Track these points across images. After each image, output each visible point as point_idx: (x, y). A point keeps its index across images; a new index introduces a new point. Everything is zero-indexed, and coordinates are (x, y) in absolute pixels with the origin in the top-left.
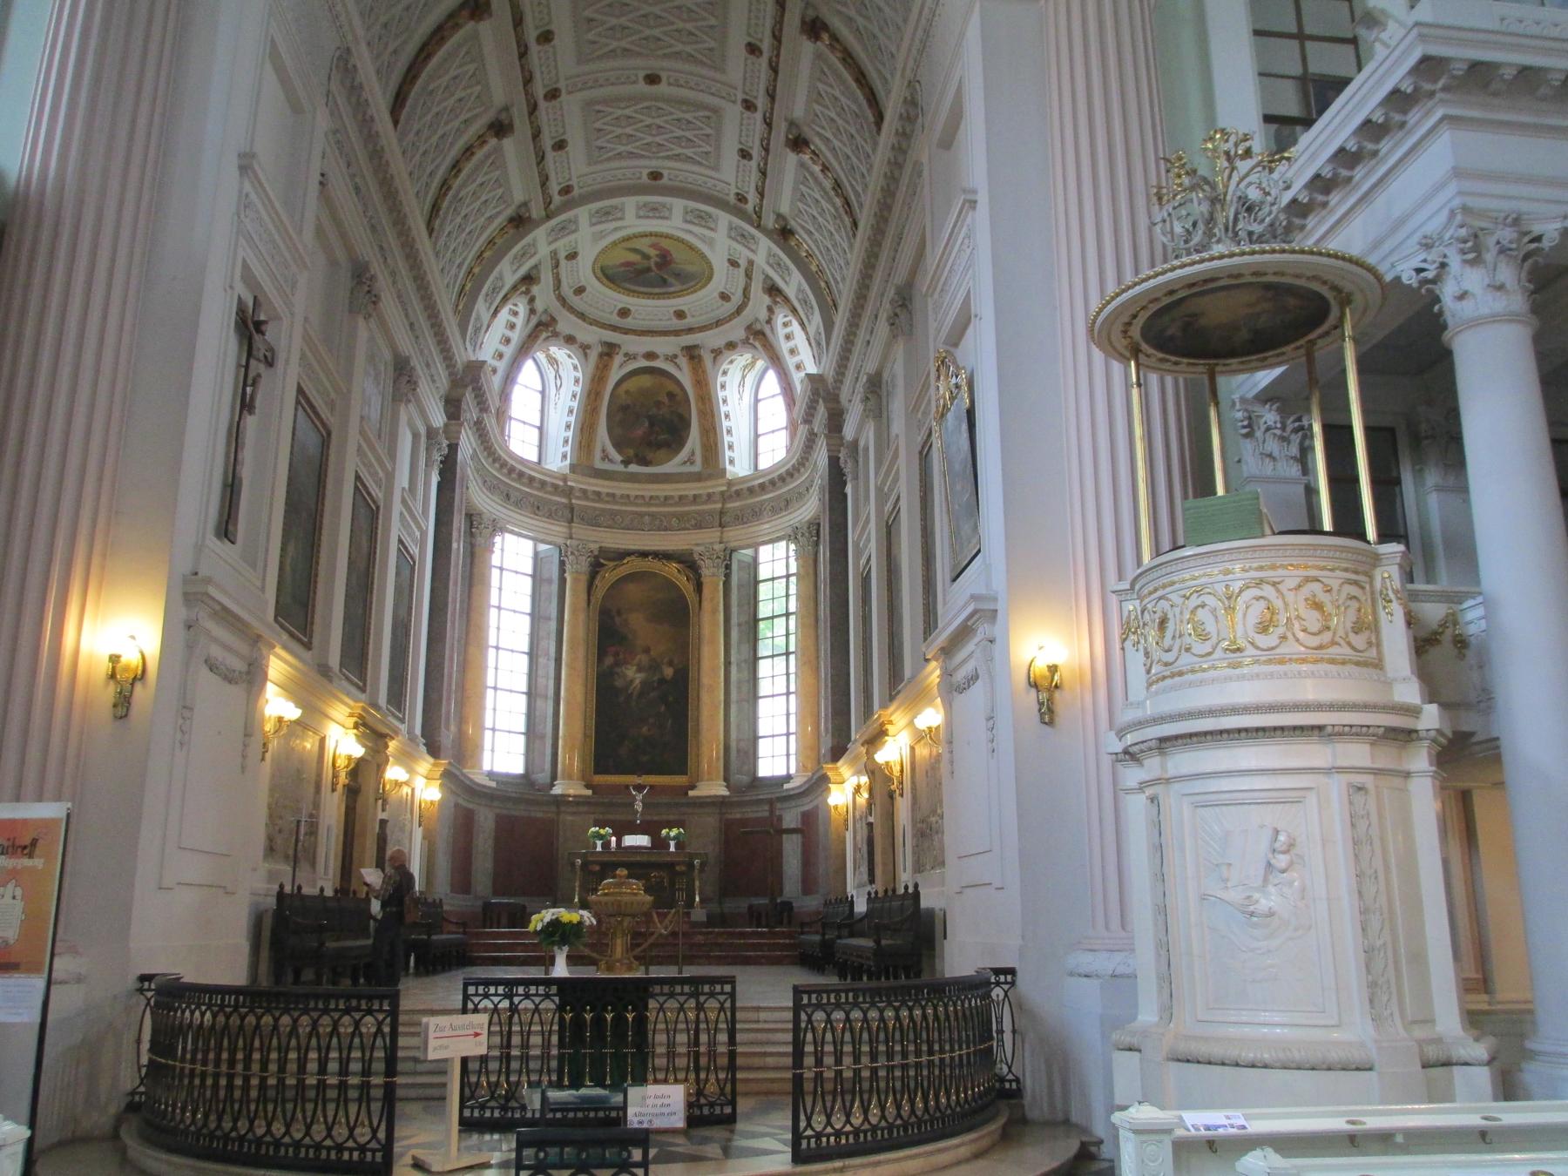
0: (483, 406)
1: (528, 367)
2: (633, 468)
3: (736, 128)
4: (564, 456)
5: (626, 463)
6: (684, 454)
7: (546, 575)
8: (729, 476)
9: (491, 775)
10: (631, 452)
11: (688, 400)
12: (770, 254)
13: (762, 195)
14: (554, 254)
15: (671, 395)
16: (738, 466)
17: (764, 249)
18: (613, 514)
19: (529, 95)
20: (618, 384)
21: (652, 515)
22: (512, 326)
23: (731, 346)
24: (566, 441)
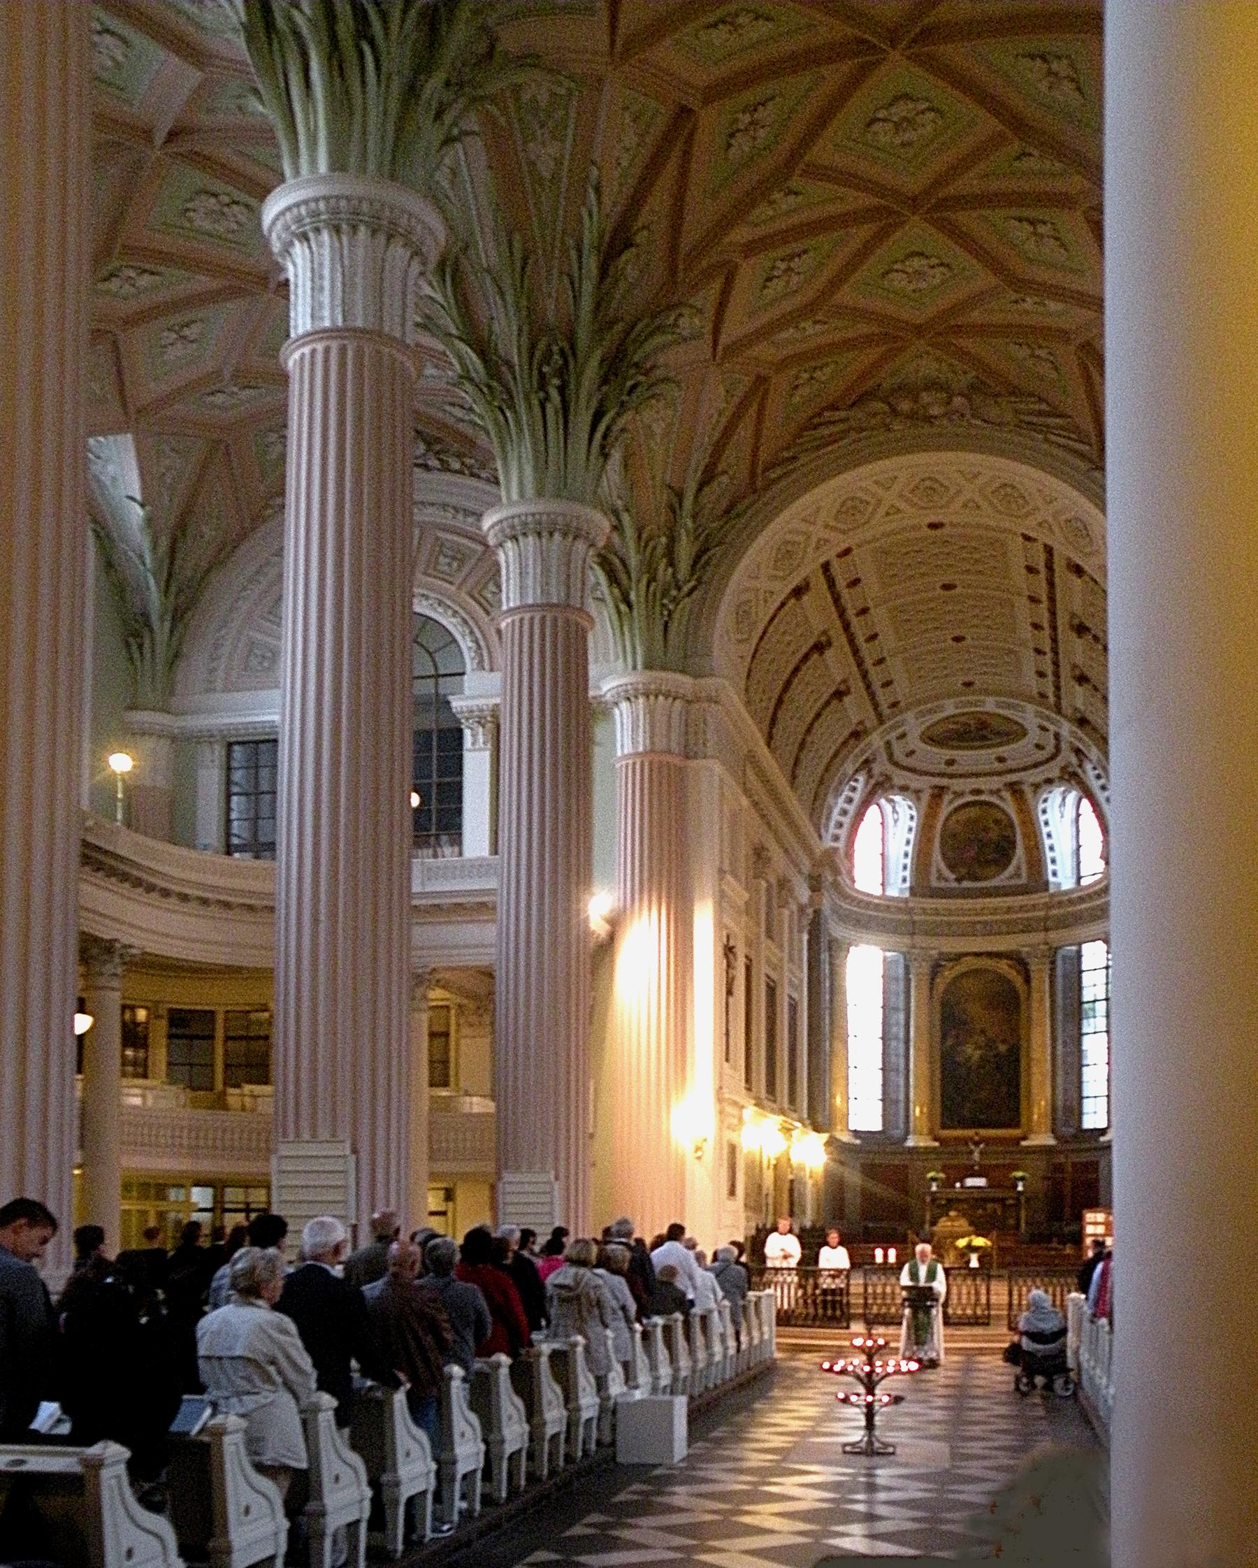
0: (836, 871)
1: (873, 811)
2: (966, 884)
3: (1029, 663)
4: (904, 880)
5: (958, 880)
6: (1011, 869)
7: (893, 1096)
8: (1052, 890)
9: (856, 1133)
10: (963, 871)
11: (1012, 825)
12: (1072, 732)
13: (1058, 697)
14: (888, 744)
15: (997, 822)
16: (1062, 878)
17: (1066, 728)
18: (949, 924)
19: (860, 664)
20: (950, 815)
21: (985, 923)
22: (854, 789)
23: (1049, 781)
24: (905, 867)
